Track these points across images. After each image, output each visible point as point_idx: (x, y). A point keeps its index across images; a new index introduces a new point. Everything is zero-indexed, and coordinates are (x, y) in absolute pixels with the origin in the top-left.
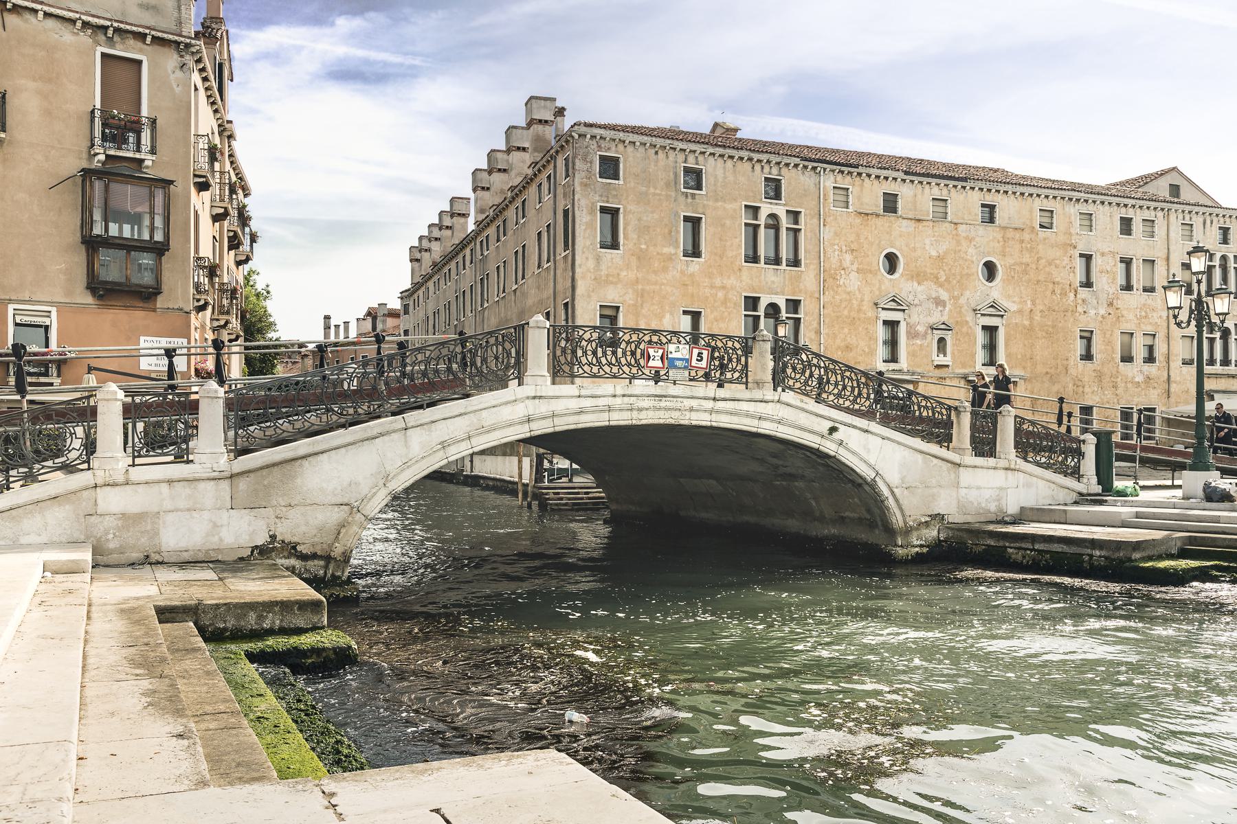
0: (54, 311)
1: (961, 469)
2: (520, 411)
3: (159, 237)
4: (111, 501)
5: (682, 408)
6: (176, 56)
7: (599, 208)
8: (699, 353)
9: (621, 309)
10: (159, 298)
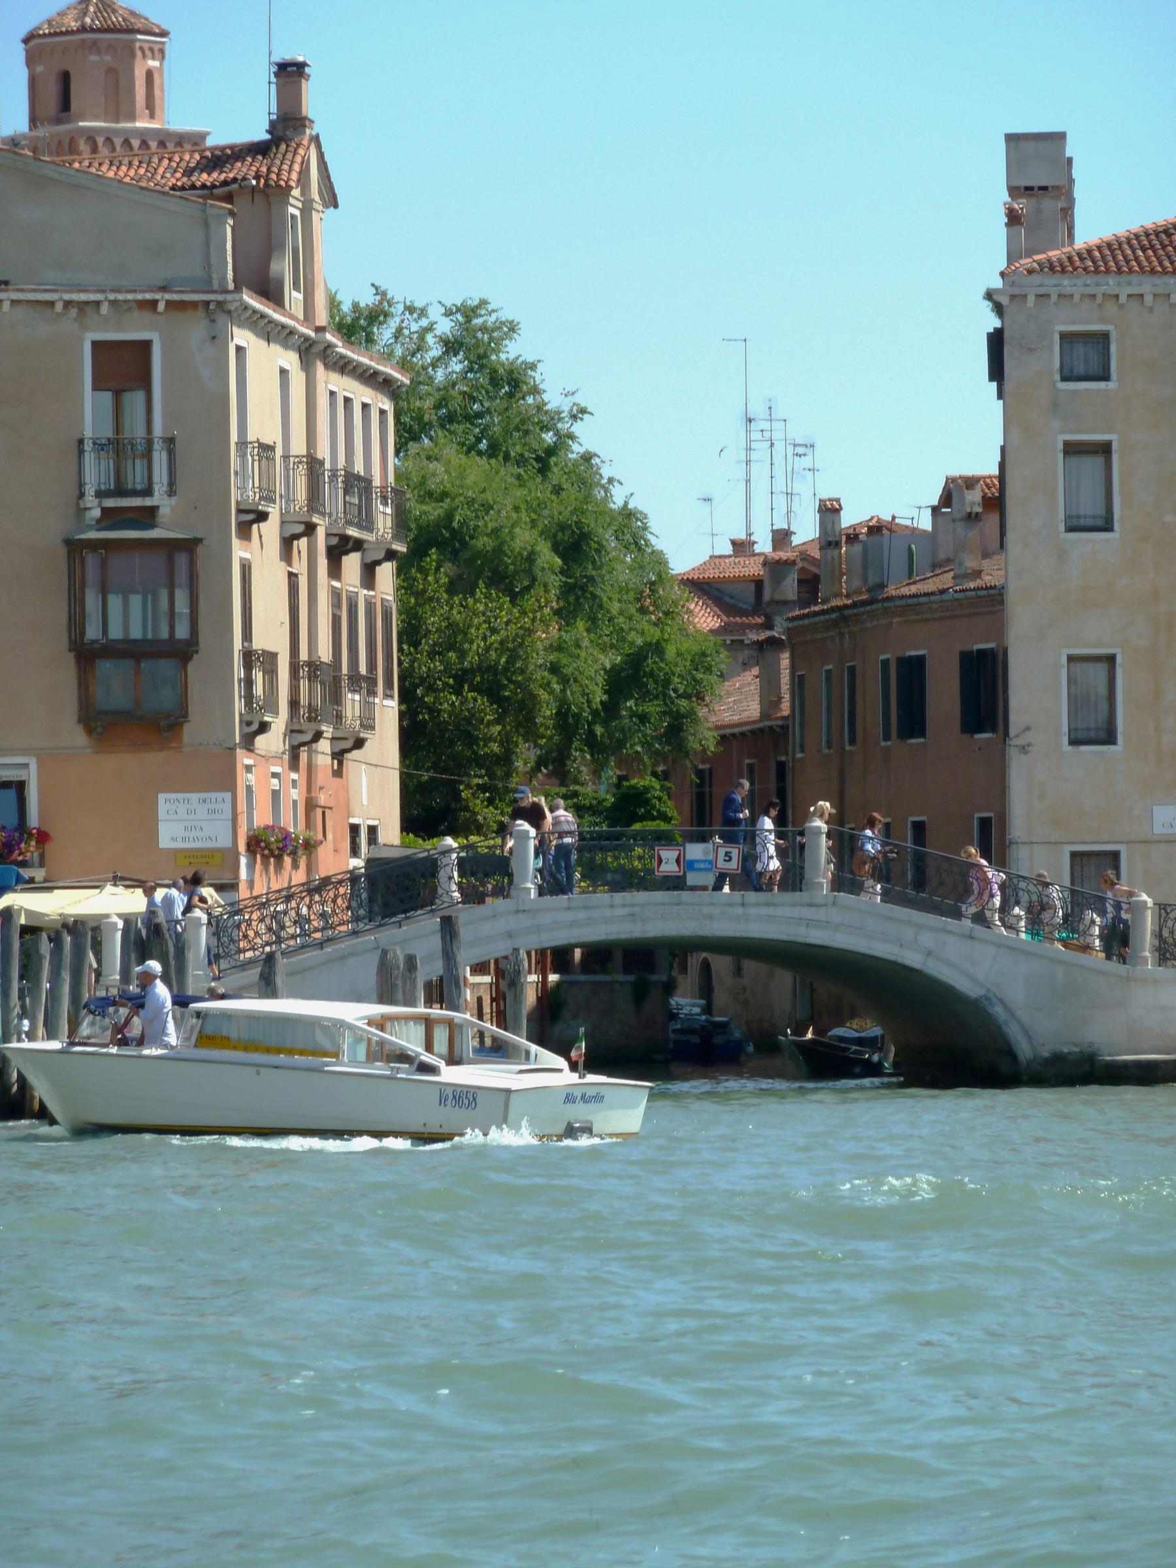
2: (501, 925)
3: (182, 632)
6: (204, 323)
7: (1060, 446)
9: (1119, 659)
10: (187, 729)
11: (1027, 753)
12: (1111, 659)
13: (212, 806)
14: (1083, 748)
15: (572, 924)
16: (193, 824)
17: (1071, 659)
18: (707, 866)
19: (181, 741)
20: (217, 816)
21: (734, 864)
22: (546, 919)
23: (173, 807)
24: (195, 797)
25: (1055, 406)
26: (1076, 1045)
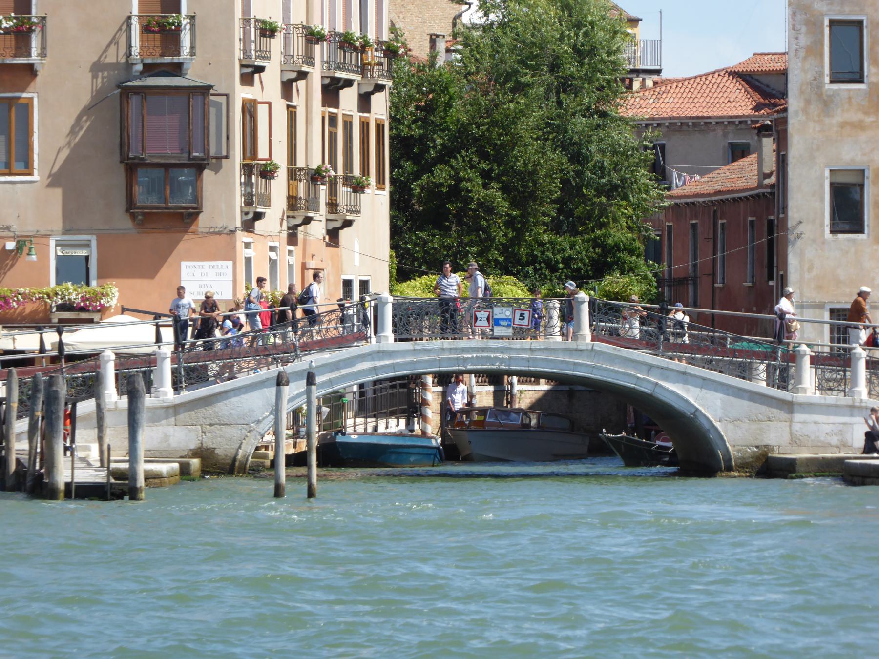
10: (201, 217)
16: (205, 283)
19: (197, 226)
20: (222, 278)
21: (526, 322)
24: (207, 264)
26: (757, 447)
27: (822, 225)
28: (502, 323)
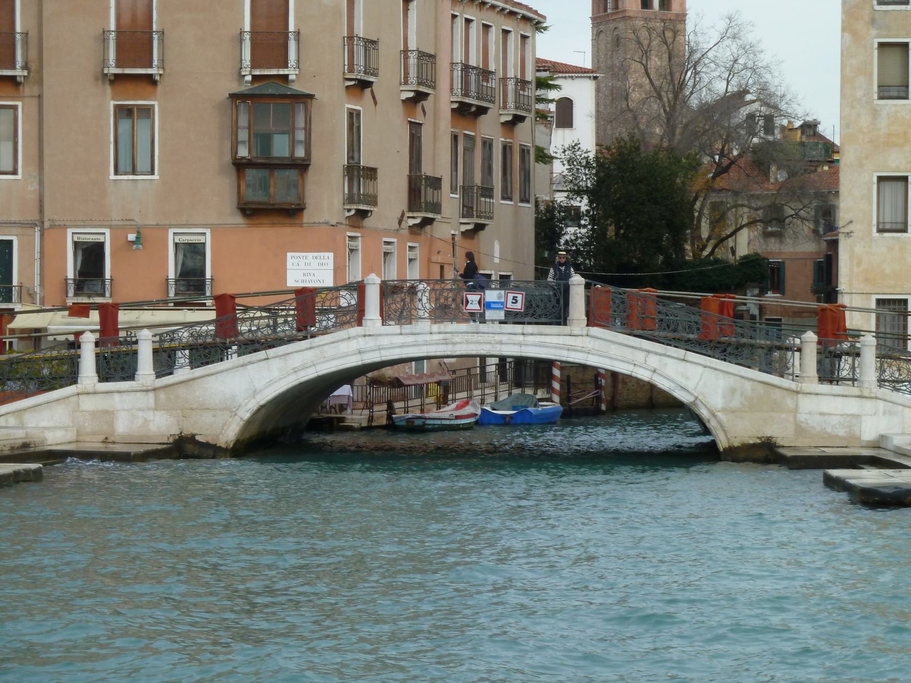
0: (208, 232)
1: (800, 396)
3: (300, 153)
4: (88, 404)
5: (493, 342)
7: (876, 46)
8: (514, 297)
11: (851, 236)
12: (905, 179)
13: (321, 261)
14: (886, 235)
15: (402, 346)
17: (881, 179)
18: (500, 306)
19: (302, 220)
20: (324, 267)
21: (519, 306)
22: (385, 341)
23: (295, 261)
24: (310, 255)
25: (873, 21)
27: (870, 225)
28: (493, 306)
